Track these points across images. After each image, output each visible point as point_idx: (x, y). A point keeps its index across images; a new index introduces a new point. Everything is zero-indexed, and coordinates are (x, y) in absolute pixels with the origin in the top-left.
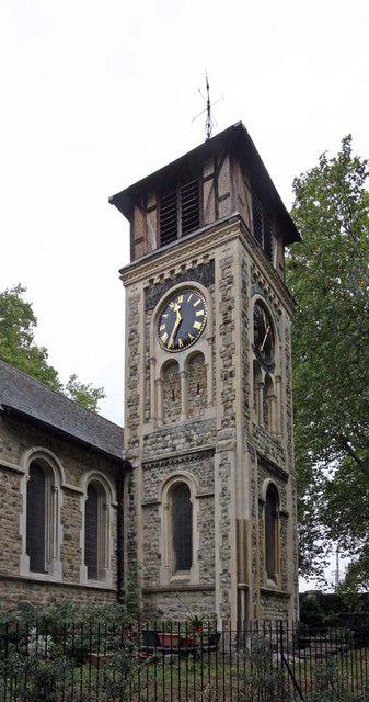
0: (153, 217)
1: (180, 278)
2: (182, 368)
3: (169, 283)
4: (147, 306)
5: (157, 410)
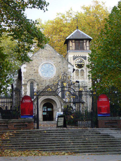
0: (74, 44)
1: (80, 57)
2: (80, 71)
3: (78, 57)
4: (73, 59)
5: (75, 78)
